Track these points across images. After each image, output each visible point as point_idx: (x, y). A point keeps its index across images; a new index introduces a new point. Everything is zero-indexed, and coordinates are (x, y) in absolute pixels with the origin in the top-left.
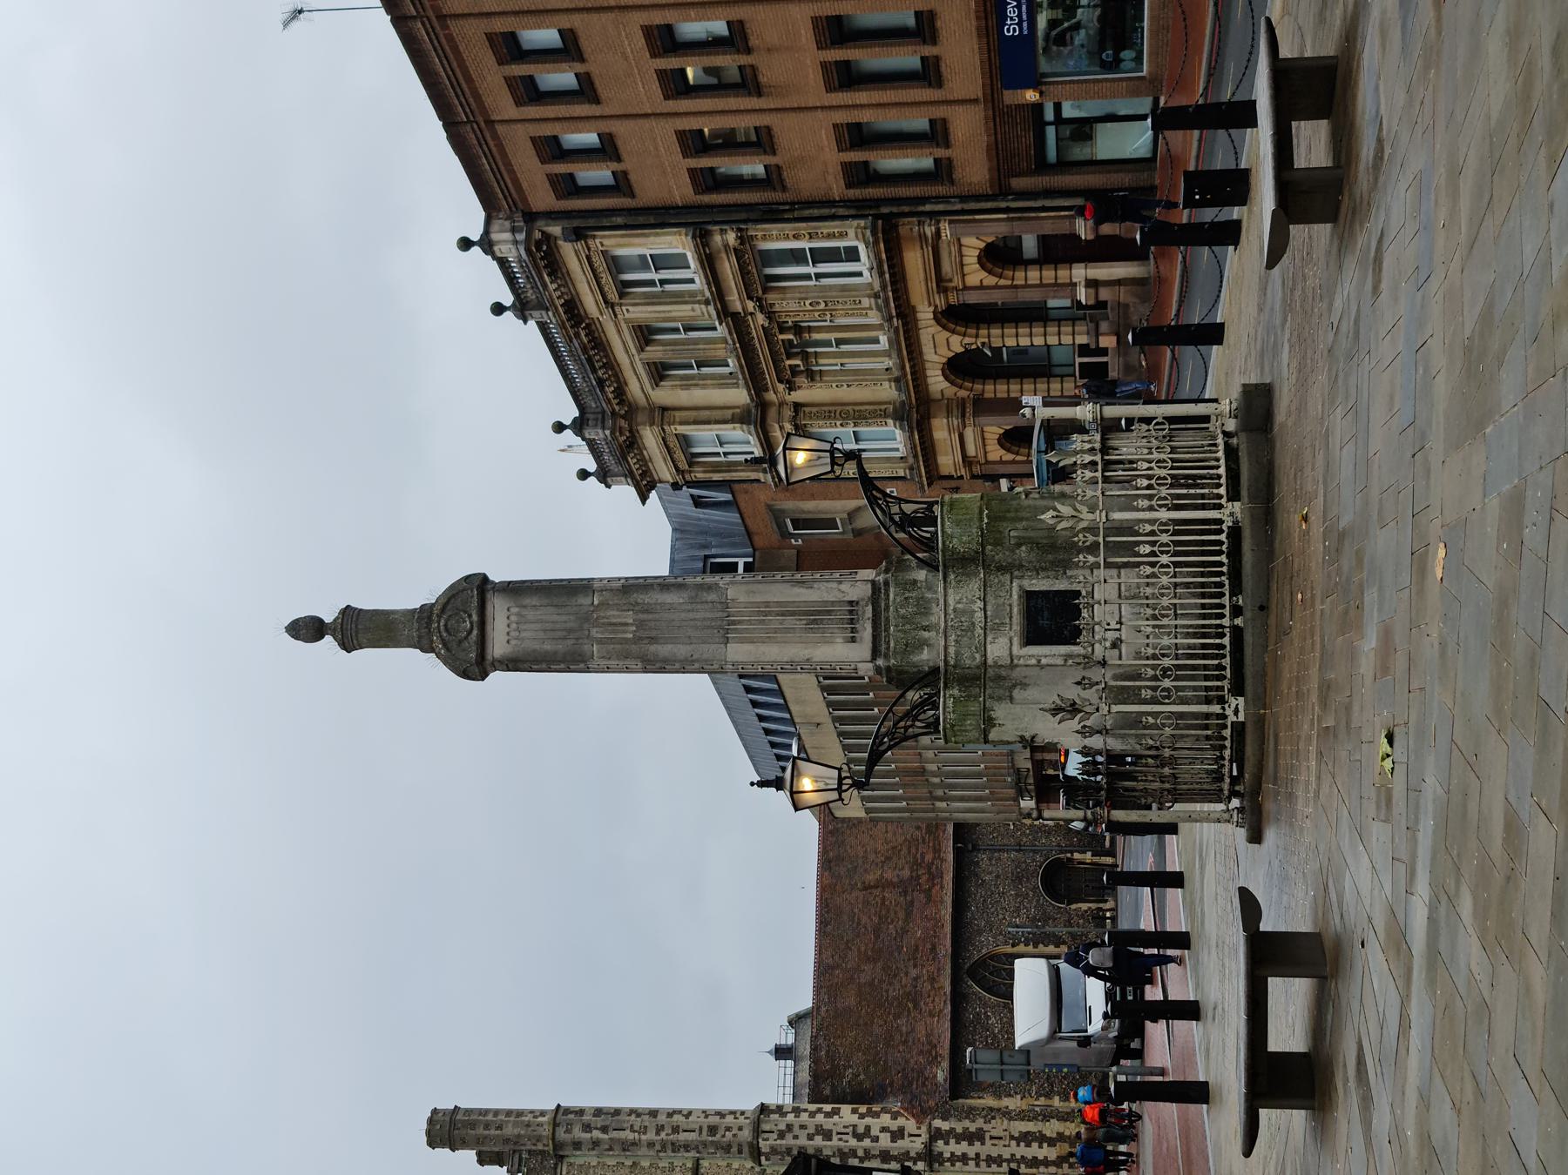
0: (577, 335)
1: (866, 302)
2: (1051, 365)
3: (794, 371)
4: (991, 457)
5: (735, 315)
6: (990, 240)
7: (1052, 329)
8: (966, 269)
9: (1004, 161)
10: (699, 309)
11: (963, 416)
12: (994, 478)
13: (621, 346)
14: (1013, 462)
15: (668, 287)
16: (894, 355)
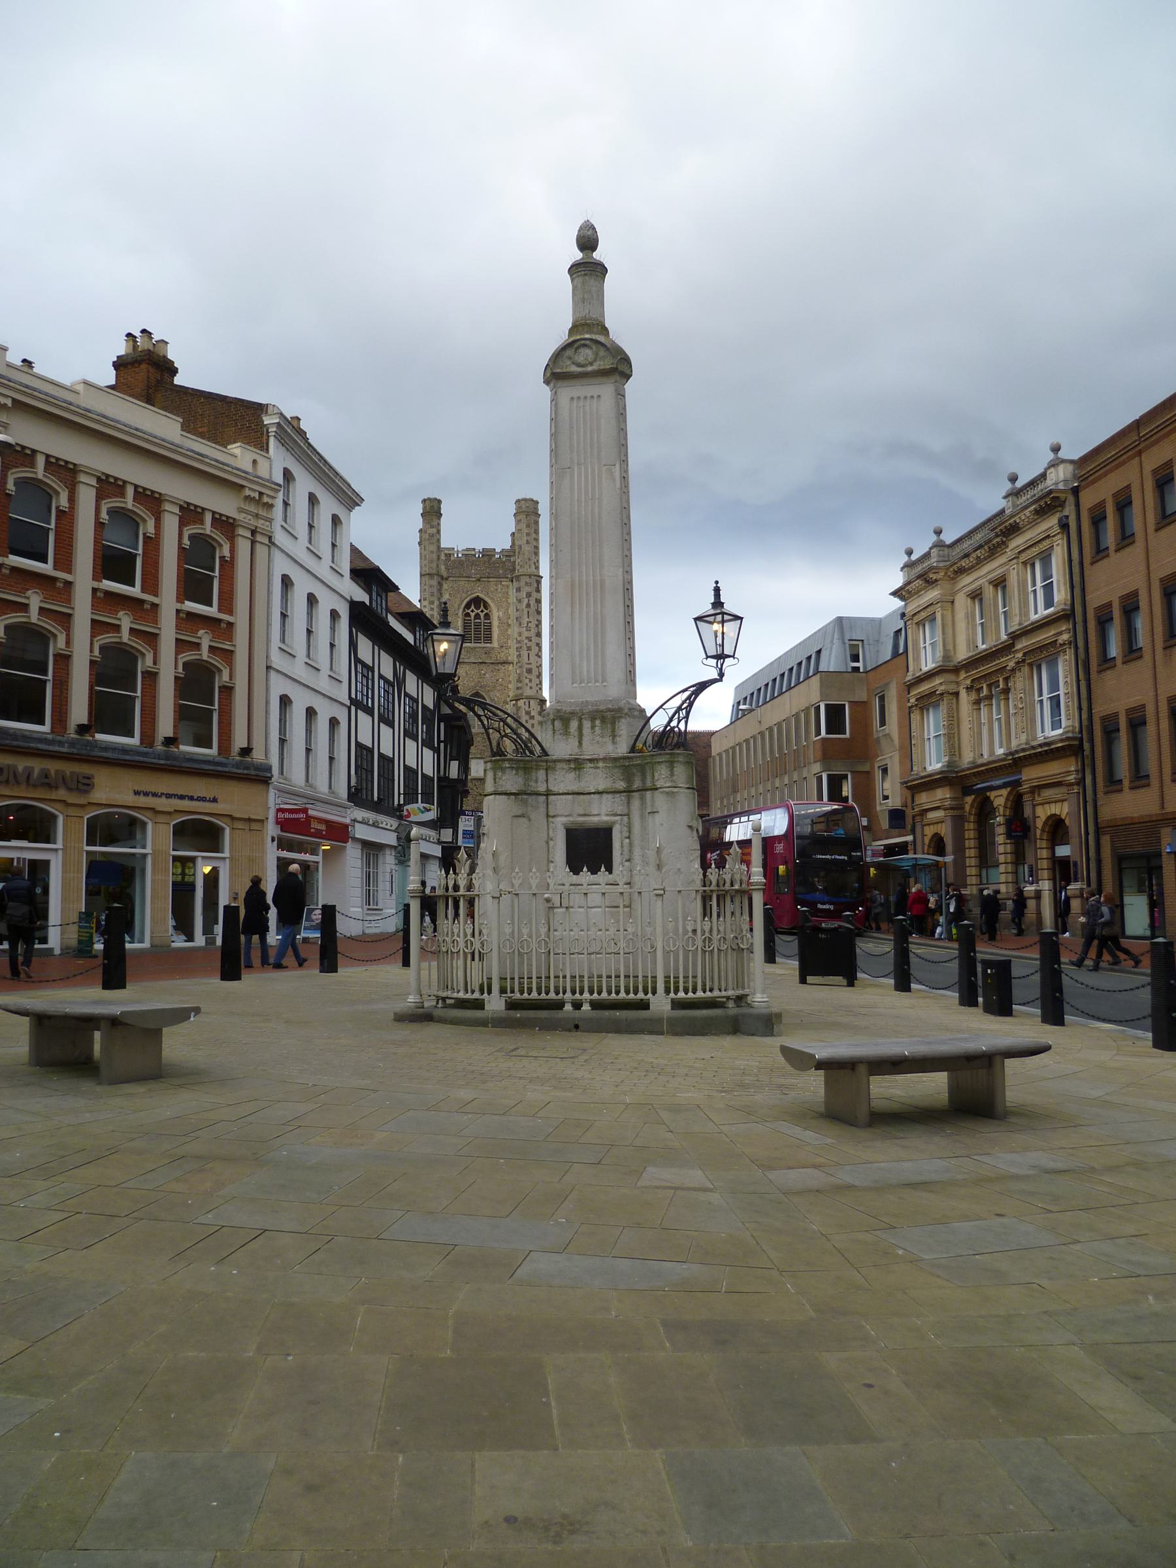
0: (997, 536)
1: (1024, 738)
2: (987, 868)
3: (980, 690)
4: (927, 829)
5: (1013, 645)
6: (1067, 822)
7: (1010, 868)
8: (1047, 806)
9: (1122, 828)
10: (1016, 620)
11: (952, 809)
12: (913, 832)
13: (992, 568)
14: (923, 844)
15: (1031, 597)
16: (991, 759)
